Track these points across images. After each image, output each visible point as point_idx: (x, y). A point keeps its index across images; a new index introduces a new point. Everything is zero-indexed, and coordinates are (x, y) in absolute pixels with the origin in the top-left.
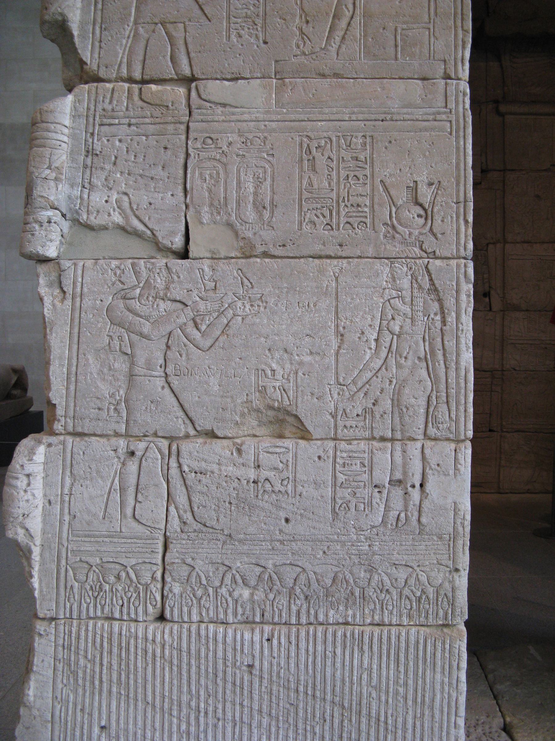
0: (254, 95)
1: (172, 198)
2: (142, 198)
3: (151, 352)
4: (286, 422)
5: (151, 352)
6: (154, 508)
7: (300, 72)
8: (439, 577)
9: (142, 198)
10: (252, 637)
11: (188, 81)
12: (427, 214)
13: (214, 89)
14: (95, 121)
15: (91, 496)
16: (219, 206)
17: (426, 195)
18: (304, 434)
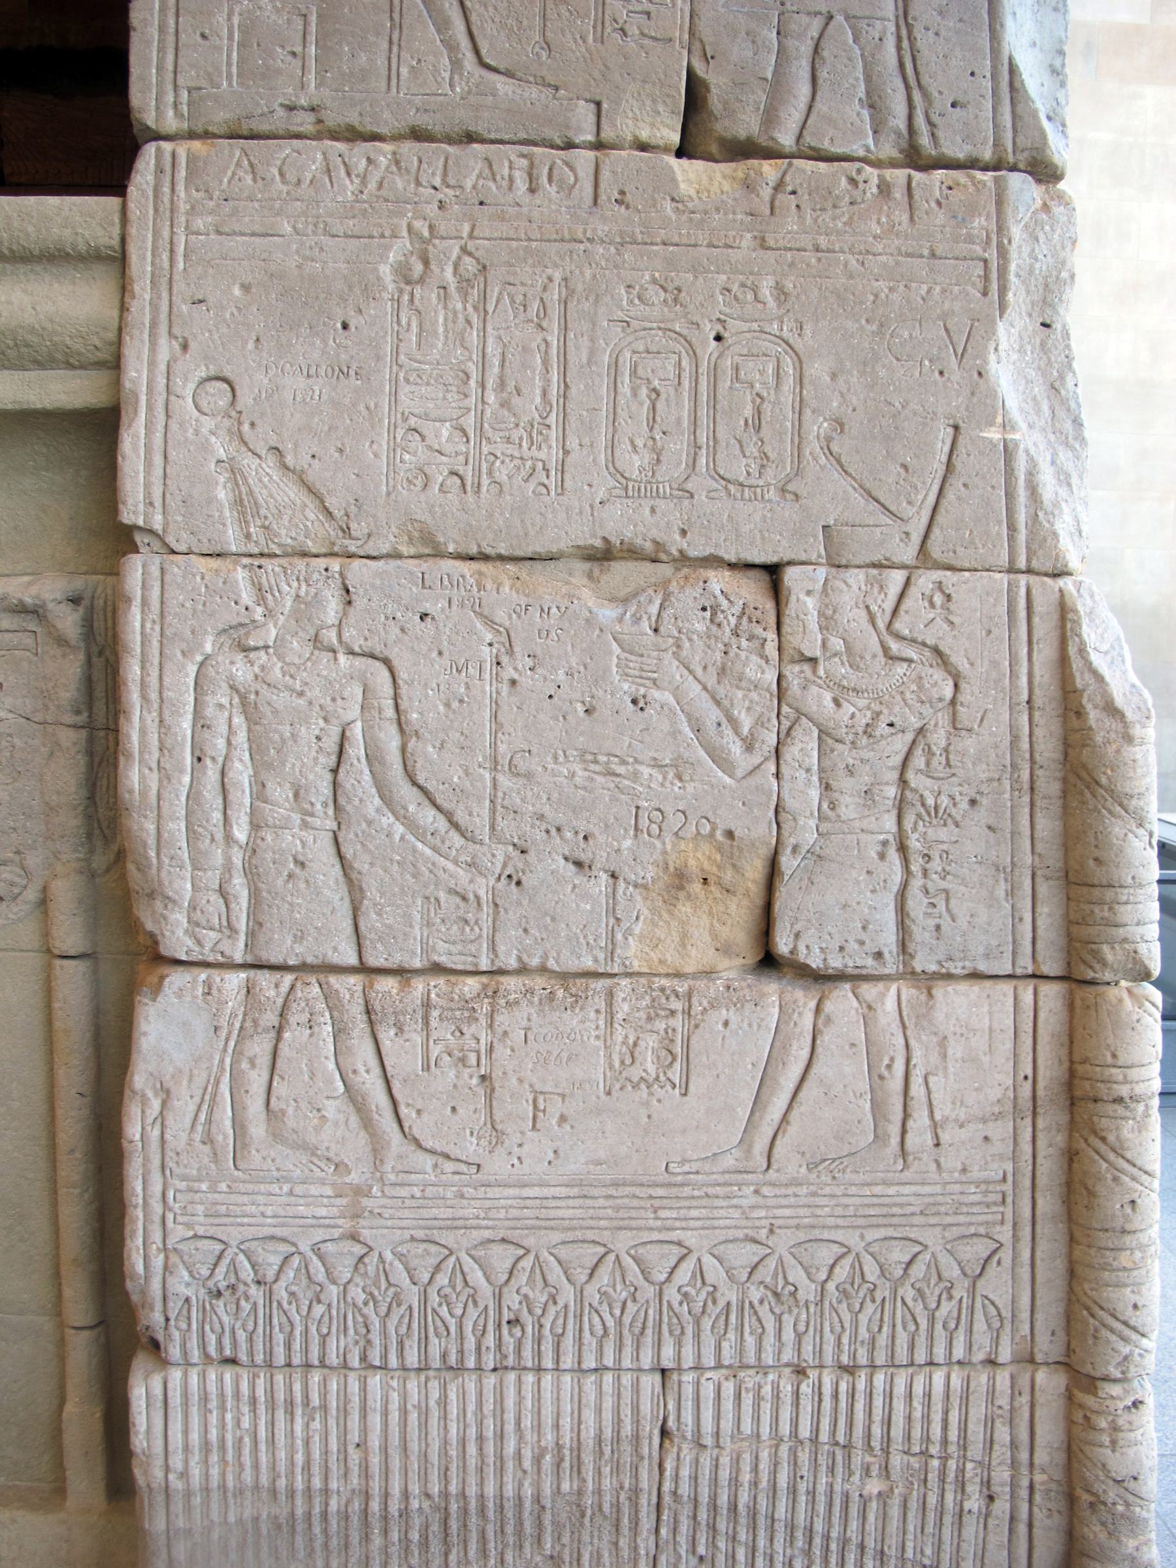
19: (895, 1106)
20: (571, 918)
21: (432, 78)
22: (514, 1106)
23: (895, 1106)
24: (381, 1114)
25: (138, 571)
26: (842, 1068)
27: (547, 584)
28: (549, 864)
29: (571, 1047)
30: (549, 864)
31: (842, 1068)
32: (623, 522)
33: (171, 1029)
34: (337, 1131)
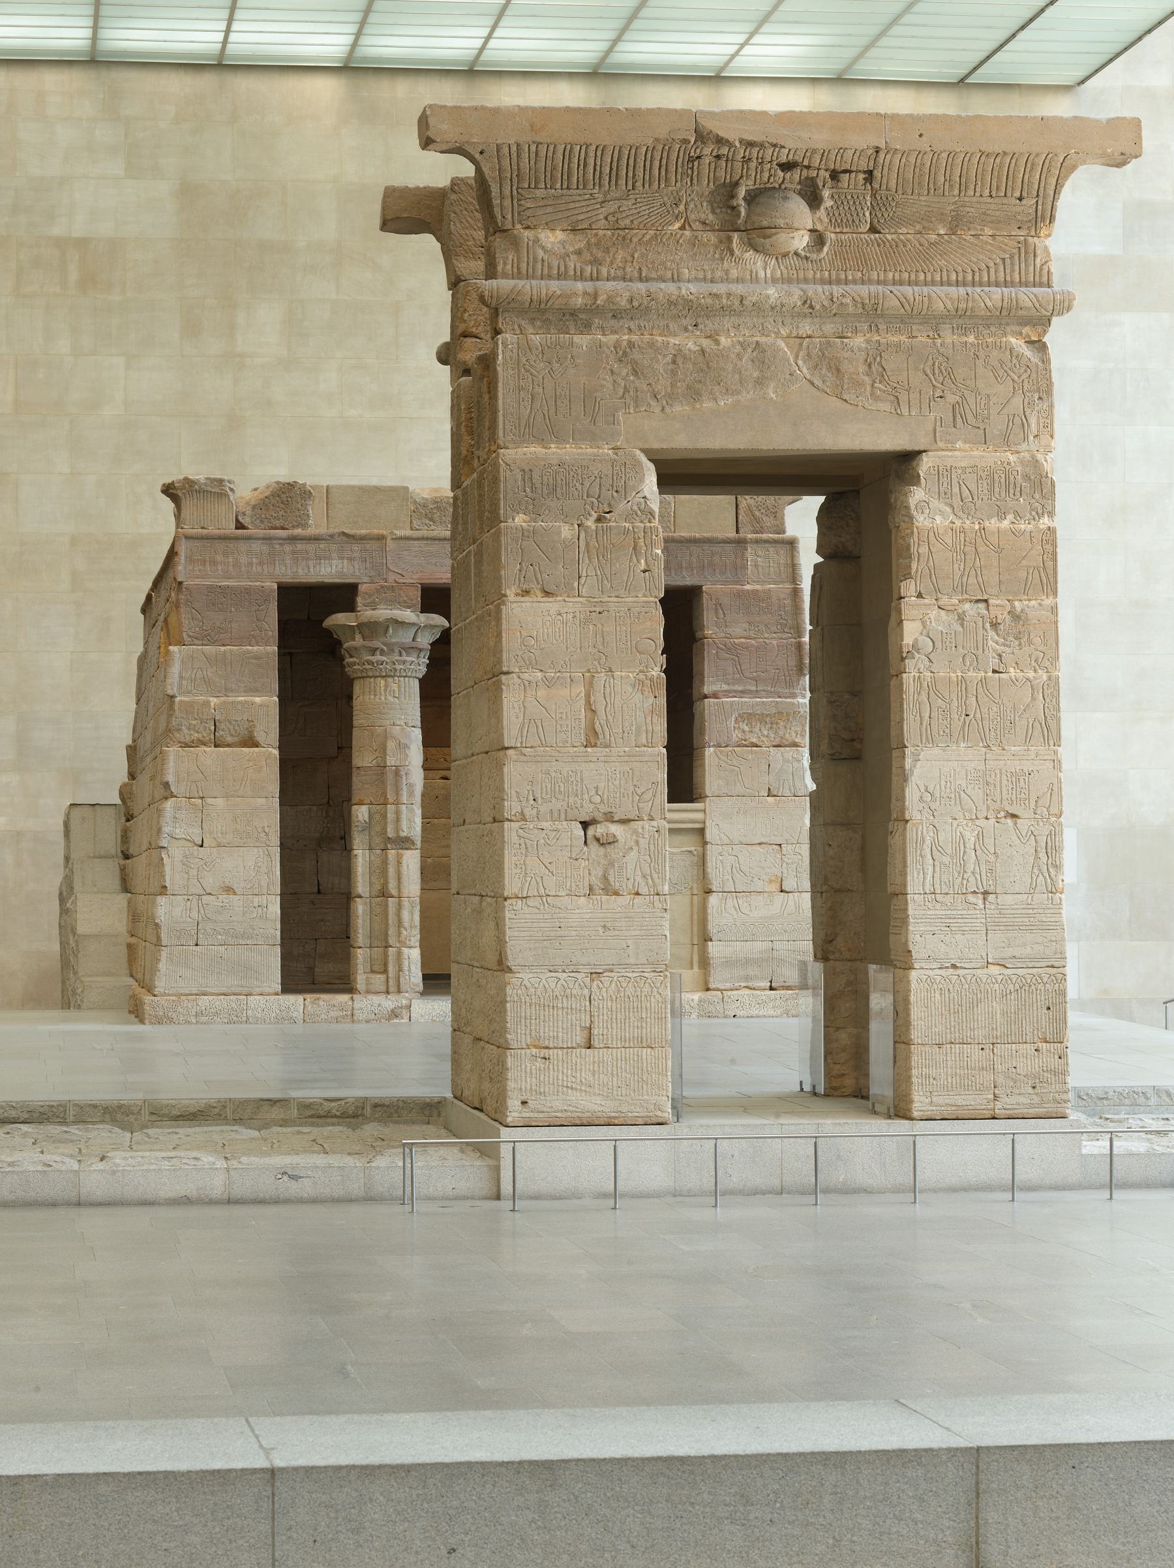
0: (220, 802)
1: (198, 831)
2: (190, 831)
3: (193, 872)
4: (229, 890)
5: (193, 872)
6: (195, 914)
7: (233, 796)
8: (272, 931)
9: (190, 831)
10: (222, 948)
11: (202, 798)
12: (267, 834)
13: (209, 801)
14: (178, 808)
15: (177, 912)
16: (211, 833)
17: (267, 830)
18: (235, 894)
19: (798, 907)
20: (759, 885)
21: (739, 789)
22: (753, 908)
23: (798, 907)
24: (738, 909)
25: (709, 846)
26: (791, 903)
27: (755, 847)
28: (756, 879)
29: (758, 900)
30: (756, 879)
31: (791, 903)
32: (763, 840)
33: (713, 900)
34: (733, 911)
